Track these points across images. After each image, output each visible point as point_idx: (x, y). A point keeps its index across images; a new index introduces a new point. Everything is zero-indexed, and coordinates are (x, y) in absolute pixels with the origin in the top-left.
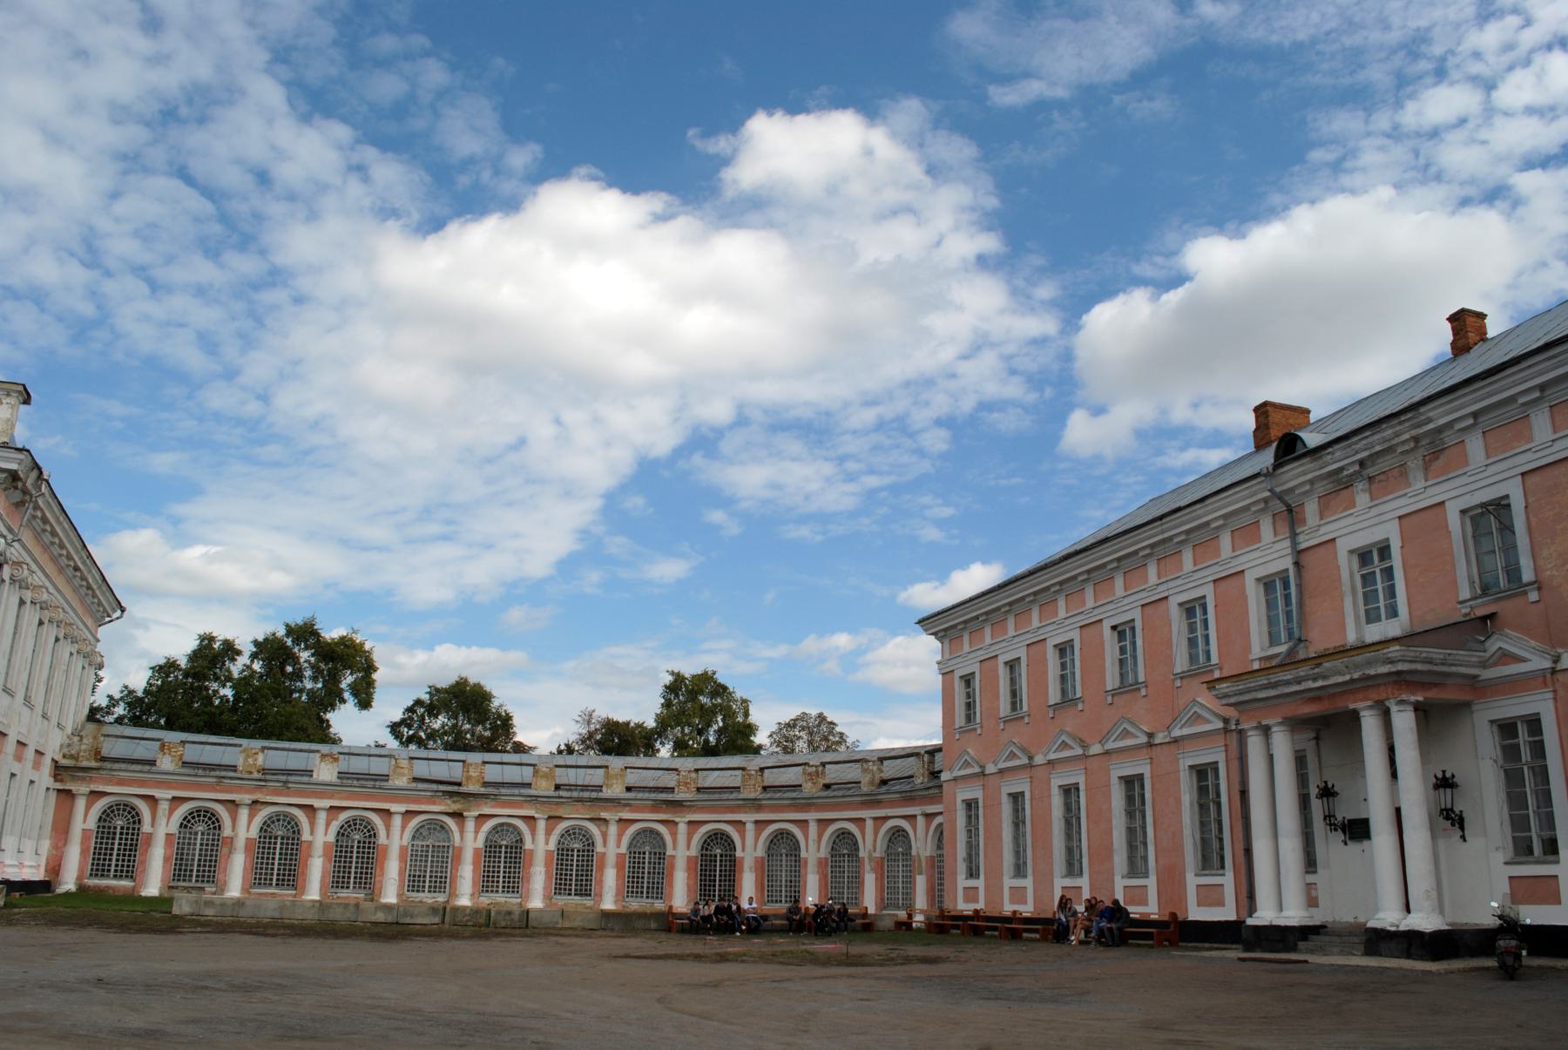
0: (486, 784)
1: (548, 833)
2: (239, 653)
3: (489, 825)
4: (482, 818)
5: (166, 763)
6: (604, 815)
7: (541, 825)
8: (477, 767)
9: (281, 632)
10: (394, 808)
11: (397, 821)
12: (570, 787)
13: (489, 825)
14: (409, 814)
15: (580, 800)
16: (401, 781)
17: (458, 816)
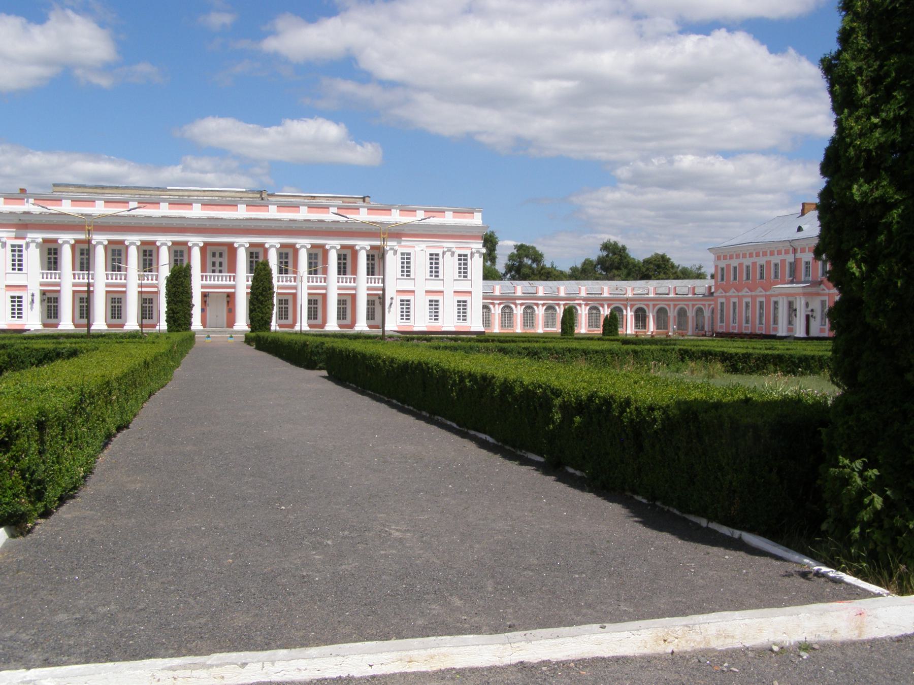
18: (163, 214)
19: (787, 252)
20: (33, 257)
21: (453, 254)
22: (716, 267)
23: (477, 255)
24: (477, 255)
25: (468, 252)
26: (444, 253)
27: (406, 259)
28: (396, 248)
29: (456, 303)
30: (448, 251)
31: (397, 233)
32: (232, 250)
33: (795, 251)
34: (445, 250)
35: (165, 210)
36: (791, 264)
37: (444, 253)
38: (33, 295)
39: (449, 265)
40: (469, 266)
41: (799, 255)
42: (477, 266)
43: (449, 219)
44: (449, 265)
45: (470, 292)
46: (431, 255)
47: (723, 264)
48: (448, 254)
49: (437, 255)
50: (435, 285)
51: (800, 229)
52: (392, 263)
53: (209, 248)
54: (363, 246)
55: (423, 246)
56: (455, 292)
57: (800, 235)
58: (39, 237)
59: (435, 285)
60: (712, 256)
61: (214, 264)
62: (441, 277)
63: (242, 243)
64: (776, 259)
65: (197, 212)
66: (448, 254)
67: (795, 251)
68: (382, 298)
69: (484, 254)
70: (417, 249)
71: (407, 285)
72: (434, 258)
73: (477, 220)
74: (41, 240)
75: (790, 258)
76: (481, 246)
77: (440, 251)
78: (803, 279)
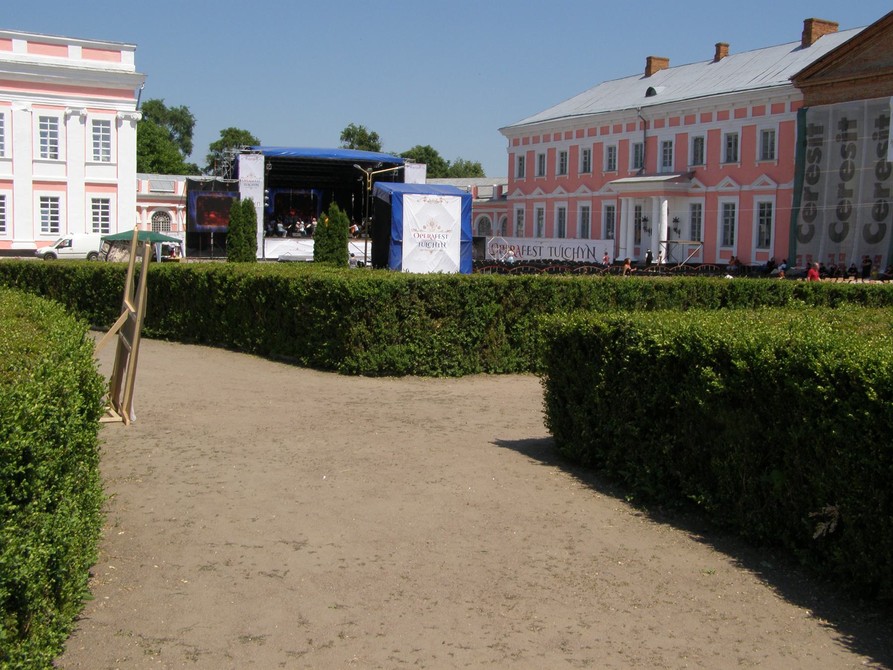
19: (631, 128)
21: (83, 119)
22: (511, 156)
23: (126, 123)
24: (126, 123)
25: (111, 118)
26: (67, 117)
29: (91, 204)
30: (75, 113)
33: (645, 125)
34: (69, 111)
36: (637, 146)
37: (67, 117)
39: (76, 139)
40: (113, 141)
41: (652, 132)
42: (126, 141)
43: (75, 58)
44: (76, 139)
45: (115, 185)
46: (43, 119)
47: (522, 151)
48: (75, 119)
49: (55, 120)
51: (650, 92)
55: (27, 102)
56: (87, 184)
57: (651, 100)
60: (505, 142)
62: (61, 158)
64: (612, 140)
66: (75, 119)
67: (645, 125)
69: (138, 122)
73: (126, 62)
75: (637, 137)
76: (133, 108)
77: (60, 114)
78: (658, 171)
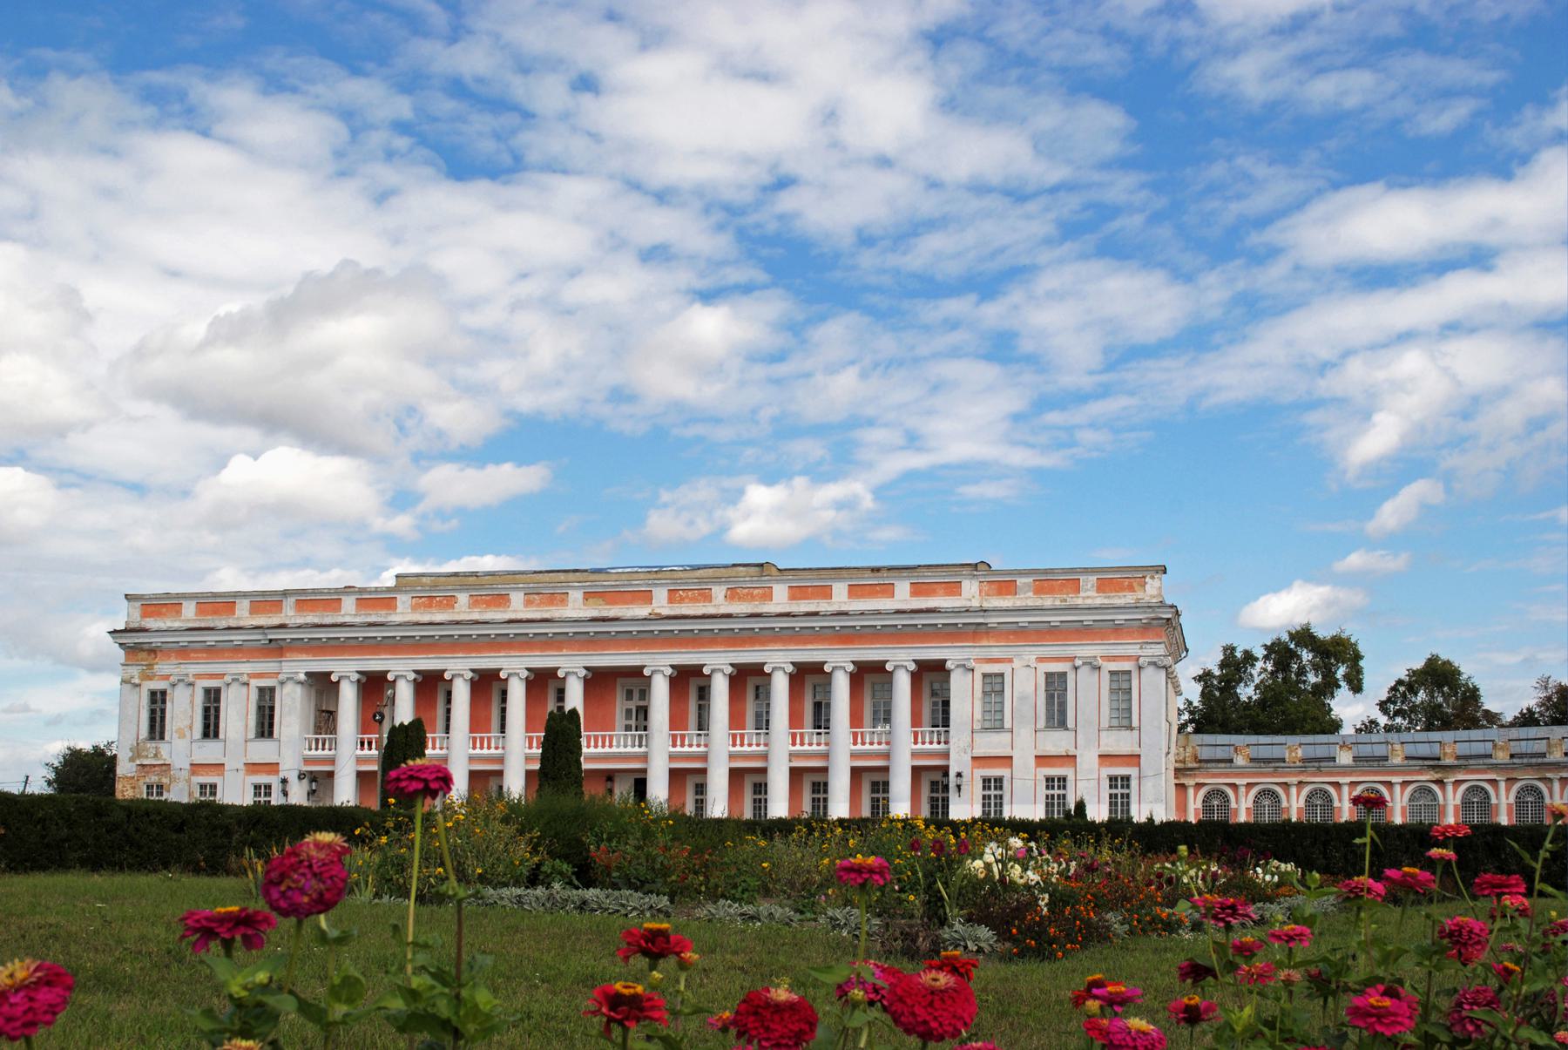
0: (1458, 758)
1: (1508, 790)
2: (1257, 659)
3: (1463, 787)
4: (1458, 783)
5: (1240, 761)
6: (1549, 775)
7: (1502, 785)
8: (1451, 743)
9: (1285, 637)
10: (1394, 779)
11: (1398, 789)
12: (1521, 756)
13: (1463, 787)
14: (1405, 784)
15: (1530, 765)
16: (1397, 760)
17: (1440, 782)
18: (513, 616)
20: (293, 709)
27: (994, 685)
28: (972, 664)
31: (972, 630)
32: (636, 678)
35: (518, 606)
38: (284, 781)
39: (1088, 695)
50: (1056, 742)
52: (964, 695)
53: (620, 681)
54: (901, 658)
58: (300, 666)
59: (1056, 742)
61: (629, 712)
62: (1070, 723)
63: (659, 664)
65: (576, 607)
68: (945, 771)
70: (1017, 664)
71: (992, 744)
72: (1056, 685)
74: (302, 677)
